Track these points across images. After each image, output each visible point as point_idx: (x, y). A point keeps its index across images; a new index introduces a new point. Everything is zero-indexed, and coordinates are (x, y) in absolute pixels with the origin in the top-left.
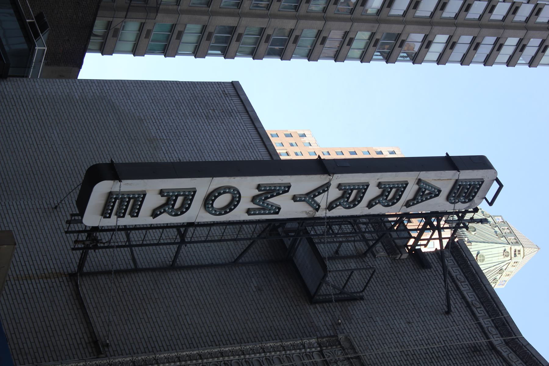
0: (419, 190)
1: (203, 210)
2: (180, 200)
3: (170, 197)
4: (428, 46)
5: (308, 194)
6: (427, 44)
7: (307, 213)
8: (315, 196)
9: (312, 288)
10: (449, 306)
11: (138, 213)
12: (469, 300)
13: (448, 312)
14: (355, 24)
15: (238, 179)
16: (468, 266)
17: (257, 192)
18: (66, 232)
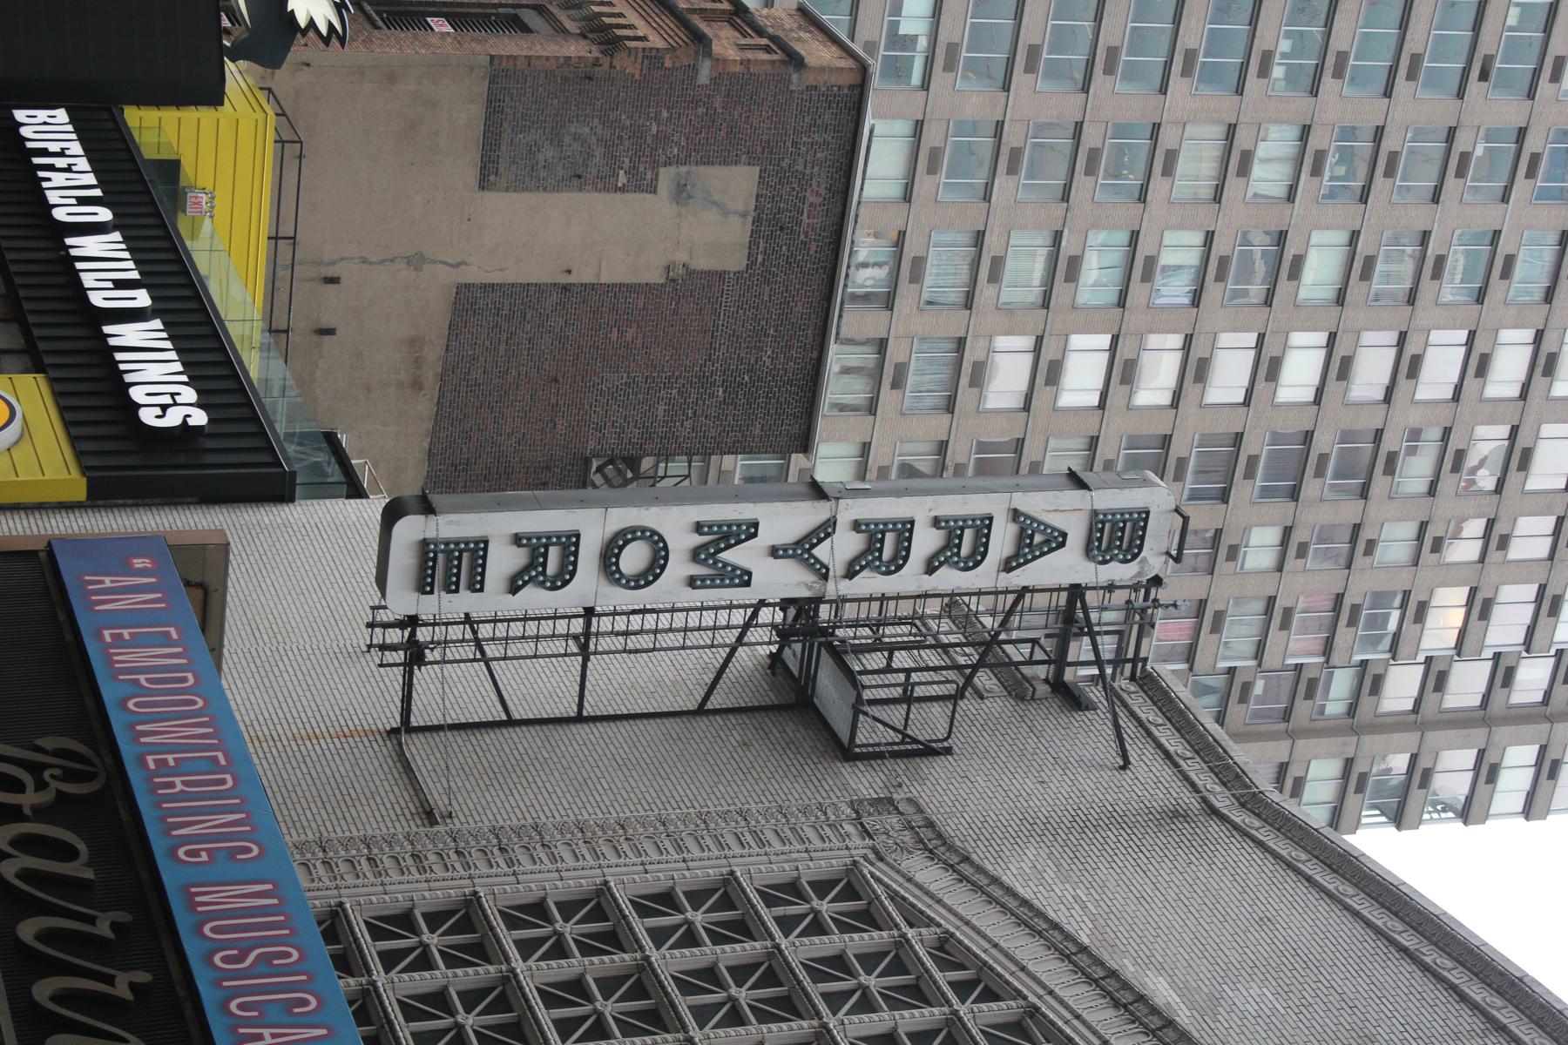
0: (1022, 530)
1: (603, 581)
2: (554, 553)
3: (534, 546)
4: (1492, 776)
5: (799, 543)
6: (1487, 772)
7: (810, 588)
8: (813, 546)
9: (843, 732)
10: (1124, 755)
11: (482, 582)
12: (1171, 749)
13: (1126, 765)
14: (1300, 743)
15: (654, 510)
16: (1171, 701)
17: (701, 539)
18: (381, 665)
